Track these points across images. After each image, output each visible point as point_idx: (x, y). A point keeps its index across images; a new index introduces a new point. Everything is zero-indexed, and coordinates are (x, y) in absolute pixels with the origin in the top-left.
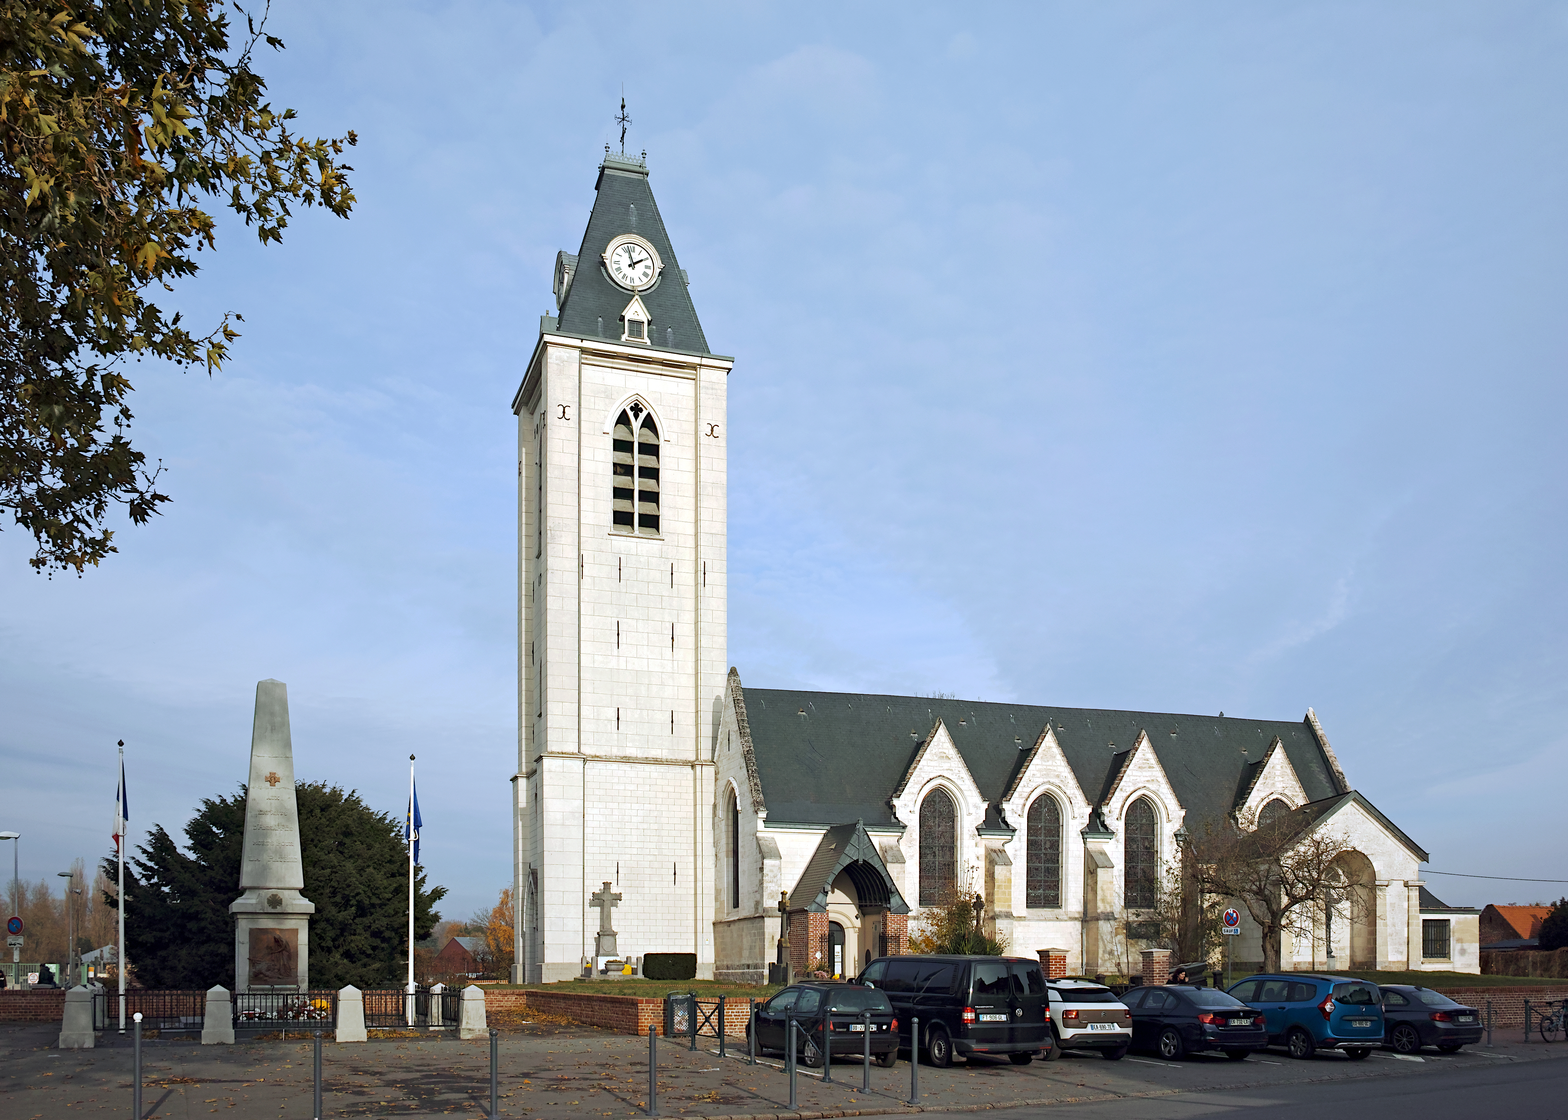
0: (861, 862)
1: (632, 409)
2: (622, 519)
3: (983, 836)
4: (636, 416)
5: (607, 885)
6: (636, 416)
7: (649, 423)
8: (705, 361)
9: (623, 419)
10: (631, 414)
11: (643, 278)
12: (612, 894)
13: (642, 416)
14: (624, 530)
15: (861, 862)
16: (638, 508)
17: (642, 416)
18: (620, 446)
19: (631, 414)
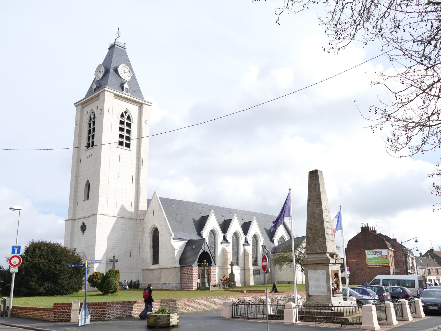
0: (205, 251)
1: (125, 112)
2: (121, 143)
3: (223, 244)
4: (126, 114)
5: (114, 257)
6: (126, 114)
7: (129, 118)
8: (145, 103)
9: (122, 116)
10: (124, 114)
11: (128, 77)
12: (115, 260)
13: (127, 115)
14: (121, 147)
15: (205, 251)
16: (125, 141)
17: (127, 115)
18: (122, 123)
19: (124, 114)
